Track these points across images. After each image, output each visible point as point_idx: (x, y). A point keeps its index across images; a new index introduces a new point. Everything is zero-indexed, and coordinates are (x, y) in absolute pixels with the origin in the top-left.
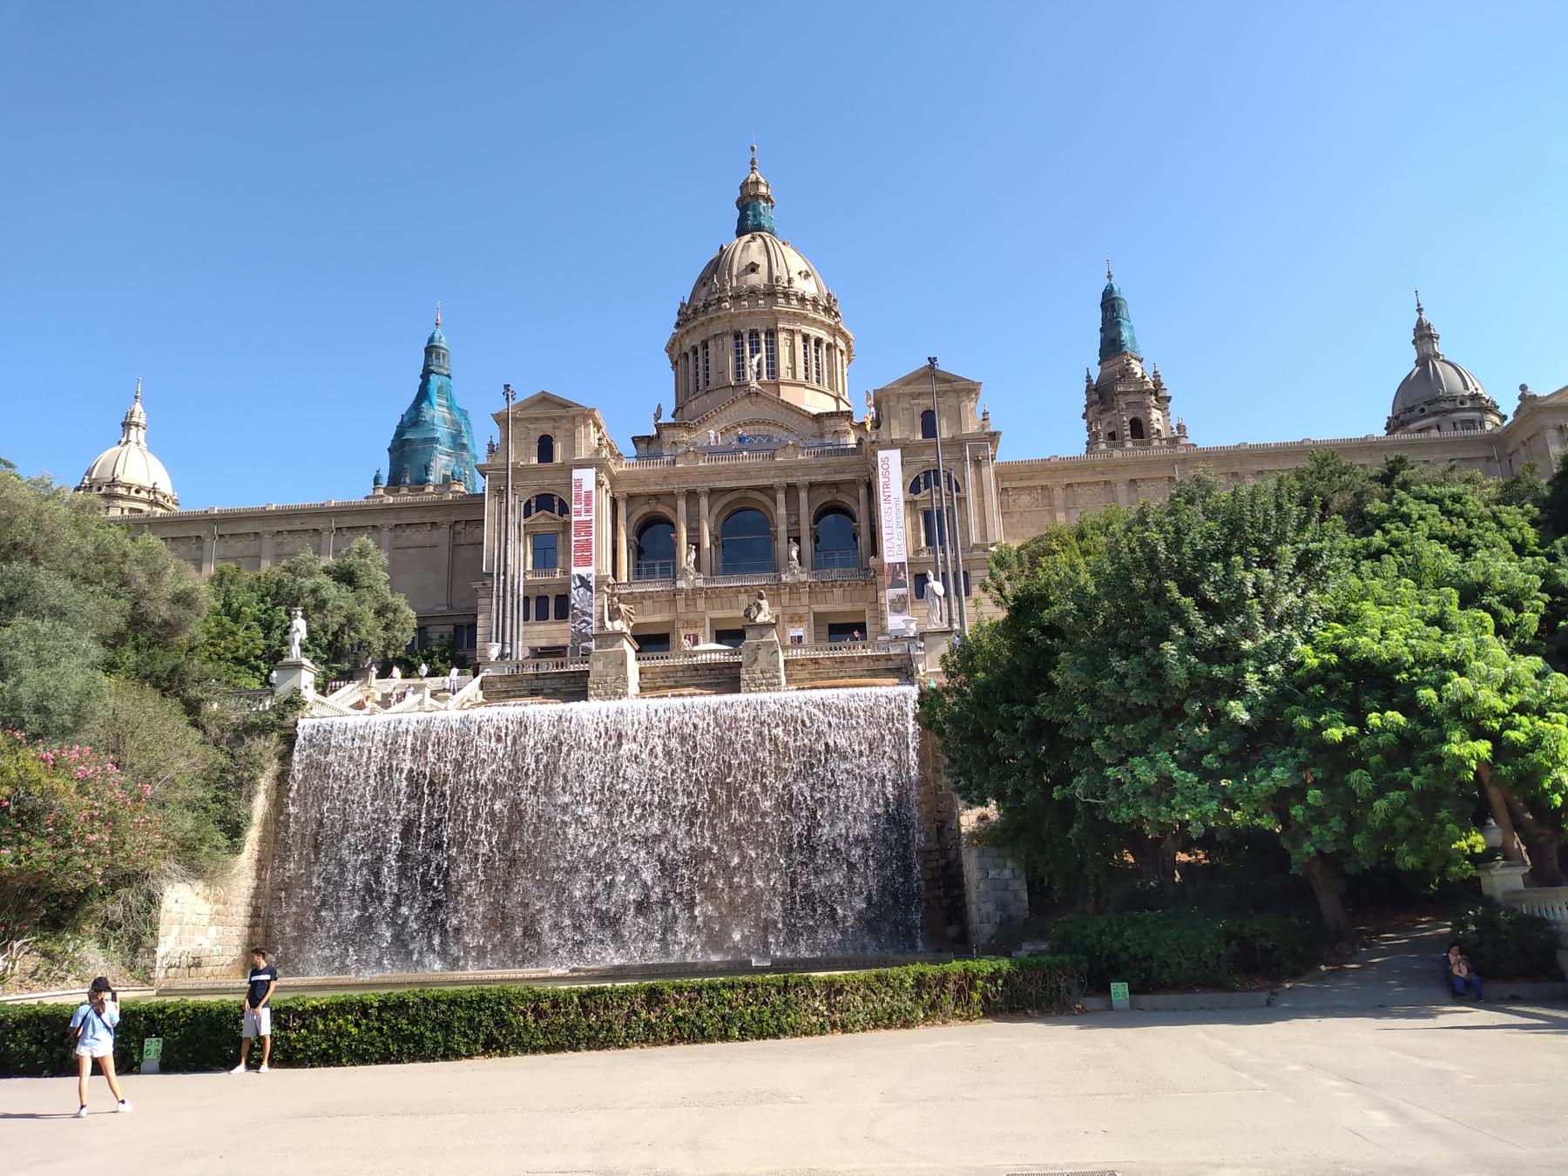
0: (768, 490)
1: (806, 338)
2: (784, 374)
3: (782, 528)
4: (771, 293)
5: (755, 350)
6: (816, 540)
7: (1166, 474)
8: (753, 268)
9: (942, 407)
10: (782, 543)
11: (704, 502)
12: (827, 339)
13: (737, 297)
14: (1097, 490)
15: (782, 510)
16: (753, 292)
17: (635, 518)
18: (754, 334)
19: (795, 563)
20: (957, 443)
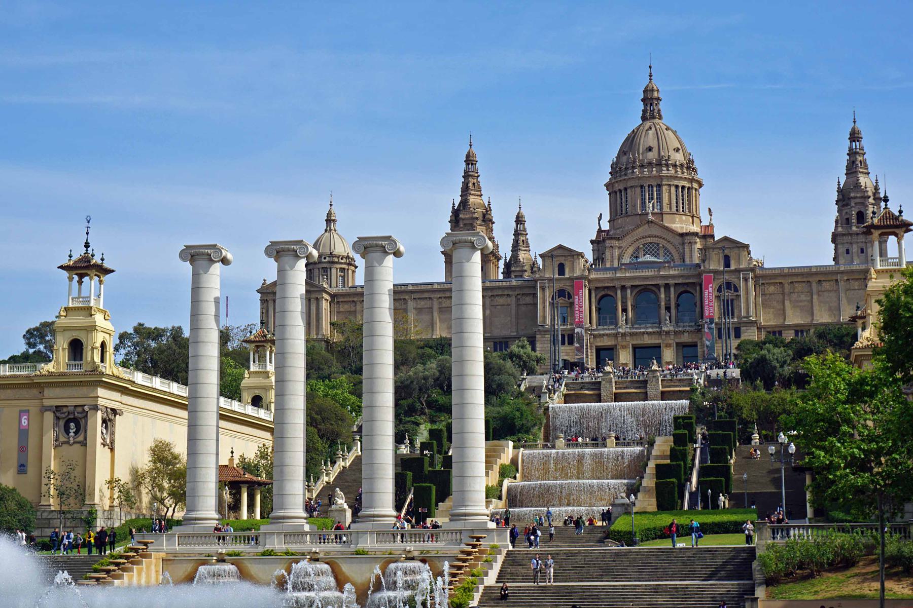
0: (657, 286)
1: (677, 187)
2: (666, 209)
3: (663, 304)
4: (659, 164)
5: (651, 198)
6: (678, 306)
7: (834, 278)
8: (650, 149)
9: (732, 254)
10: (663, 311)
11: (629, 291)
12: (687, 185)
13: (642, 166)
14: (804, 285)
15: (663, 296)
16: (650, 164)
17: (598, 297)
18: (650, 186)
19: (668, 322)
20: (738, 271)
